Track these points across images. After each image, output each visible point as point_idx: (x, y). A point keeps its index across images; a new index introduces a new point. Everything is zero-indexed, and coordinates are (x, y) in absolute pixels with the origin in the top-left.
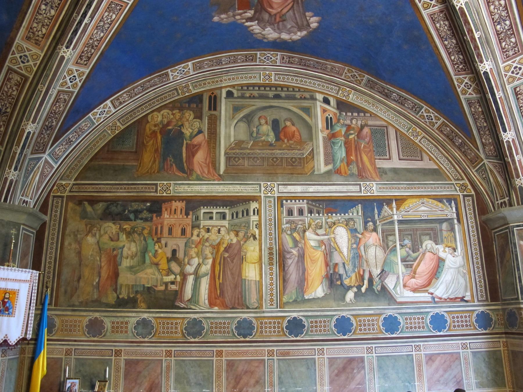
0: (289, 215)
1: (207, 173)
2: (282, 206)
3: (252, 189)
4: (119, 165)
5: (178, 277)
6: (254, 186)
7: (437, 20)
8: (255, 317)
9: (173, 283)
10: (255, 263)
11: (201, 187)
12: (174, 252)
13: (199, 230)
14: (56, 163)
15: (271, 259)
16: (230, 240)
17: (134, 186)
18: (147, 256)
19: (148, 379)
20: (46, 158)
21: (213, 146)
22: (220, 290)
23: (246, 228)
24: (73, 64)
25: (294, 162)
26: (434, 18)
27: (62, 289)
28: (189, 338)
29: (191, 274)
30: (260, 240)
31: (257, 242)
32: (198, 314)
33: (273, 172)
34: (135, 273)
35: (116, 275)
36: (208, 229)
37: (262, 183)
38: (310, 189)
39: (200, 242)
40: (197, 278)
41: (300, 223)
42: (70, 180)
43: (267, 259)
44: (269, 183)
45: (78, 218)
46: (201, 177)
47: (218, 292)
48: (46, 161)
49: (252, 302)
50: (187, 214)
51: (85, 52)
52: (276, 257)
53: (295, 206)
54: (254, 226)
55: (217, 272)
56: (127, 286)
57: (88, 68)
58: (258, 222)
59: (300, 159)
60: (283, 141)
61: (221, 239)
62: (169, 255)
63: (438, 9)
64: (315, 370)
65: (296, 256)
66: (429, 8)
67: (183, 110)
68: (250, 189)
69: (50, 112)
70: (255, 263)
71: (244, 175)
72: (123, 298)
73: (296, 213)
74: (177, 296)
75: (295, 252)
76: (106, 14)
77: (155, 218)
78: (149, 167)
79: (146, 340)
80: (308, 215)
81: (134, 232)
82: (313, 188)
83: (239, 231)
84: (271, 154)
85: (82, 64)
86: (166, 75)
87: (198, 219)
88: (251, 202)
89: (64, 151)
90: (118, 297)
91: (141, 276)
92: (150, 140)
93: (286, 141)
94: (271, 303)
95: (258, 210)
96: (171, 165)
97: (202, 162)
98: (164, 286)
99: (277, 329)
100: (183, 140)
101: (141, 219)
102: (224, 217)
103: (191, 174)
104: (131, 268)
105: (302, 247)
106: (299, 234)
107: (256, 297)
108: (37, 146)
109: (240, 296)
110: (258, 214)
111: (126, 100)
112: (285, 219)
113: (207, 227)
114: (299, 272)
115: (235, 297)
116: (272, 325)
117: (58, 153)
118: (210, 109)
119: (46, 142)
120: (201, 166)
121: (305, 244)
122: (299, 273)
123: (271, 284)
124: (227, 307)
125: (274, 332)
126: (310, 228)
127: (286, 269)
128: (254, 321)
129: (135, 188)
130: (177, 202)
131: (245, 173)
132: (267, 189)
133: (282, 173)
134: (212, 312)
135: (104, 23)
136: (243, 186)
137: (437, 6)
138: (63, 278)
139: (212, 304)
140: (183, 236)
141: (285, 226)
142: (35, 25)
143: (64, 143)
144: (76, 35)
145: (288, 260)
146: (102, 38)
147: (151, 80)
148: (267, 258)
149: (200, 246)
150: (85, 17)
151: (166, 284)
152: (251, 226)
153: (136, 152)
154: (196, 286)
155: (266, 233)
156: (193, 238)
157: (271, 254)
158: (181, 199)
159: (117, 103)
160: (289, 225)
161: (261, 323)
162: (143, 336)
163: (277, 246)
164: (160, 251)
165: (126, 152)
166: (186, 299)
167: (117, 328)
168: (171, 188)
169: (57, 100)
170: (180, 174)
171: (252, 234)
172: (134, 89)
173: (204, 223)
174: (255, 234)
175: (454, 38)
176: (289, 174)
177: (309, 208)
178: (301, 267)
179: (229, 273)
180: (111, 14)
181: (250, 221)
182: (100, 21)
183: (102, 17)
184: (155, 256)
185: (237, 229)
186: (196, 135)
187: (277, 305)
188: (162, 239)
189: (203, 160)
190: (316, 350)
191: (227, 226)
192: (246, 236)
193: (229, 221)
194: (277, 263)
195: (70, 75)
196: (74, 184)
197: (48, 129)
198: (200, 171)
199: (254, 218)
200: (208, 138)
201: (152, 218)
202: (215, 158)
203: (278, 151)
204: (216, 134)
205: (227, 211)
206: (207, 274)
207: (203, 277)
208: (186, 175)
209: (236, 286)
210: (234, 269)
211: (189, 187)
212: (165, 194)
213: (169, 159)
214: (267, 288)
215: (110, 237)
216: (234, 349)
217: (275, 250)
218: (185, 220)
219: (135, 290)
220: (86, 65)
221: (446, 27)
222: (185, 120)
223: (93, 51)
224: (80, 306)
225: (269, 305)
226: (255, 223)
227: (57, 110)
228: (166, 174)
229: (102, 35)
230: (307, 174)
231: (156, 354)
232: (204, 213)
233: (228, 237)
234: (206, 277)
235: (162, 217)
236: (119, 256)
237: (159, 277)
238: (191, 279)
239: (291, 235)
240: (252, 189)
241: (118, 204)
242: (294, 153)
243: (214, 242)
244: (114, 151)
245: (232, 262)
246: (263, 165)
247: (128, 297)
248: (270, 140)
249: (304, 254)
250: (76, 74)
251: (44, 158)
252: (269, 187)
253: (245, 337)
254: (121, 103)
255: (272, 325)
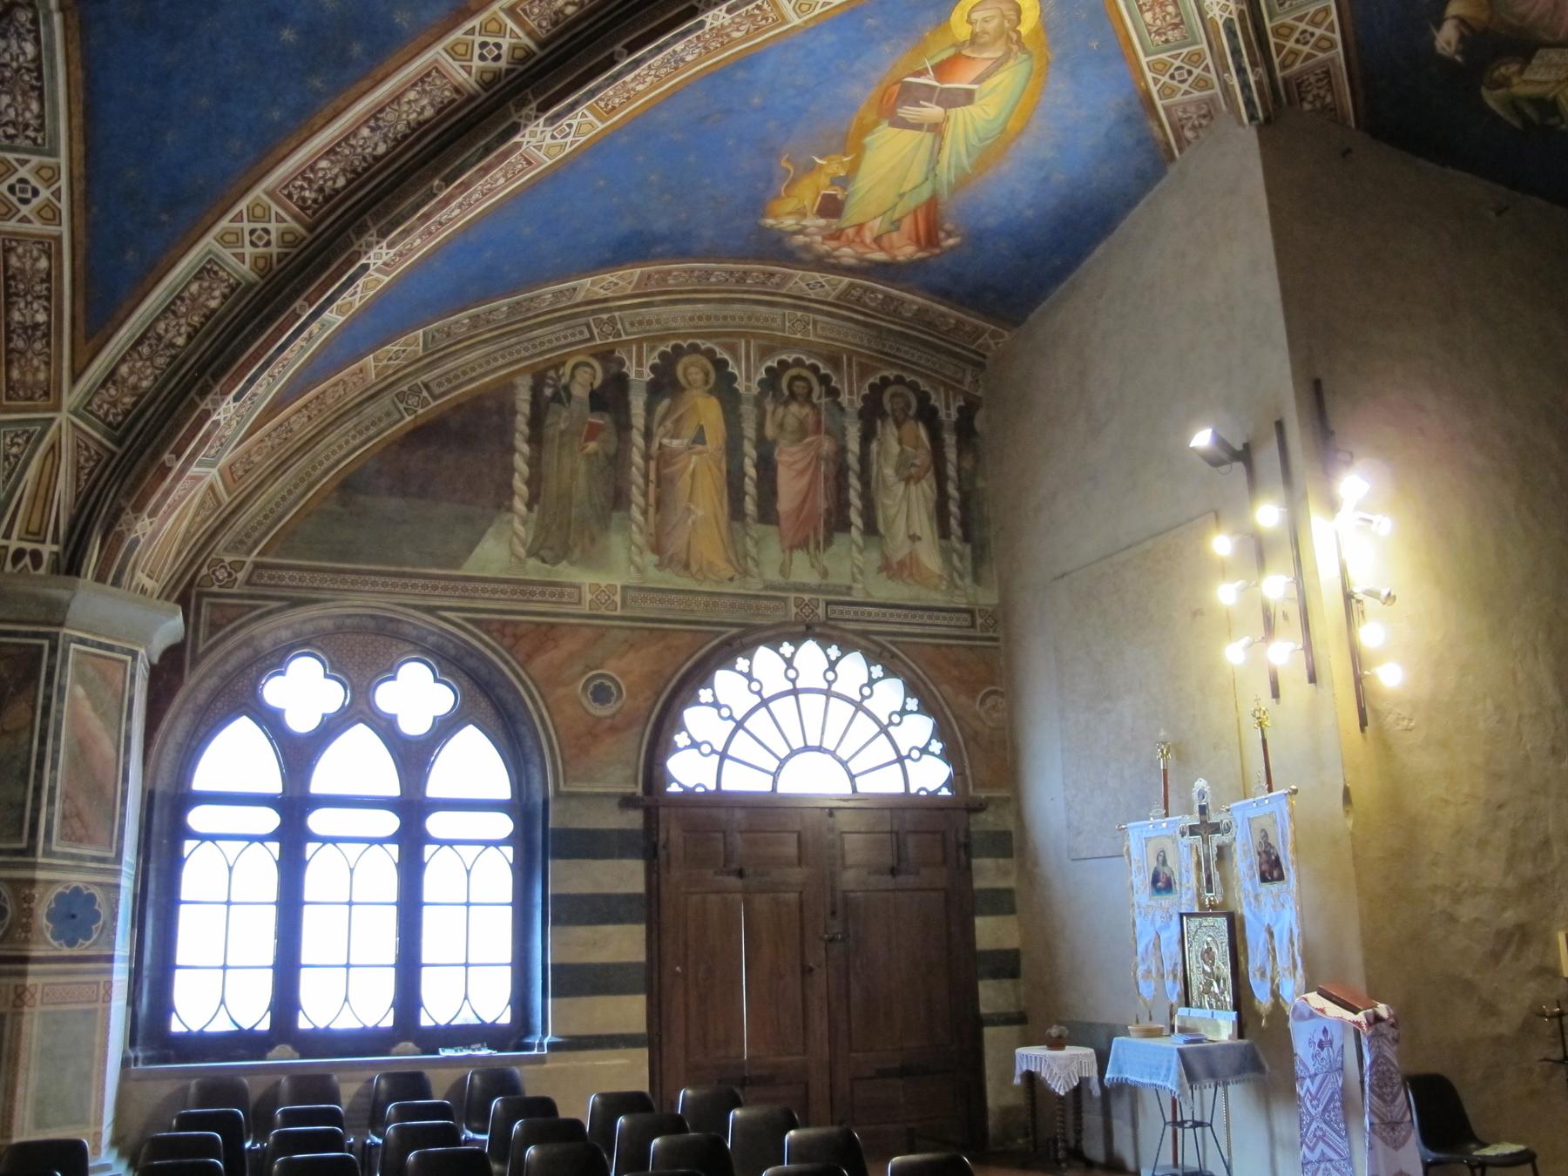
7: (428, 88)
26: (430, 80)
63: (460, 79)
66: (454, 59)
137: (470, 73)
175: (391, 144)
221: (414, 116)
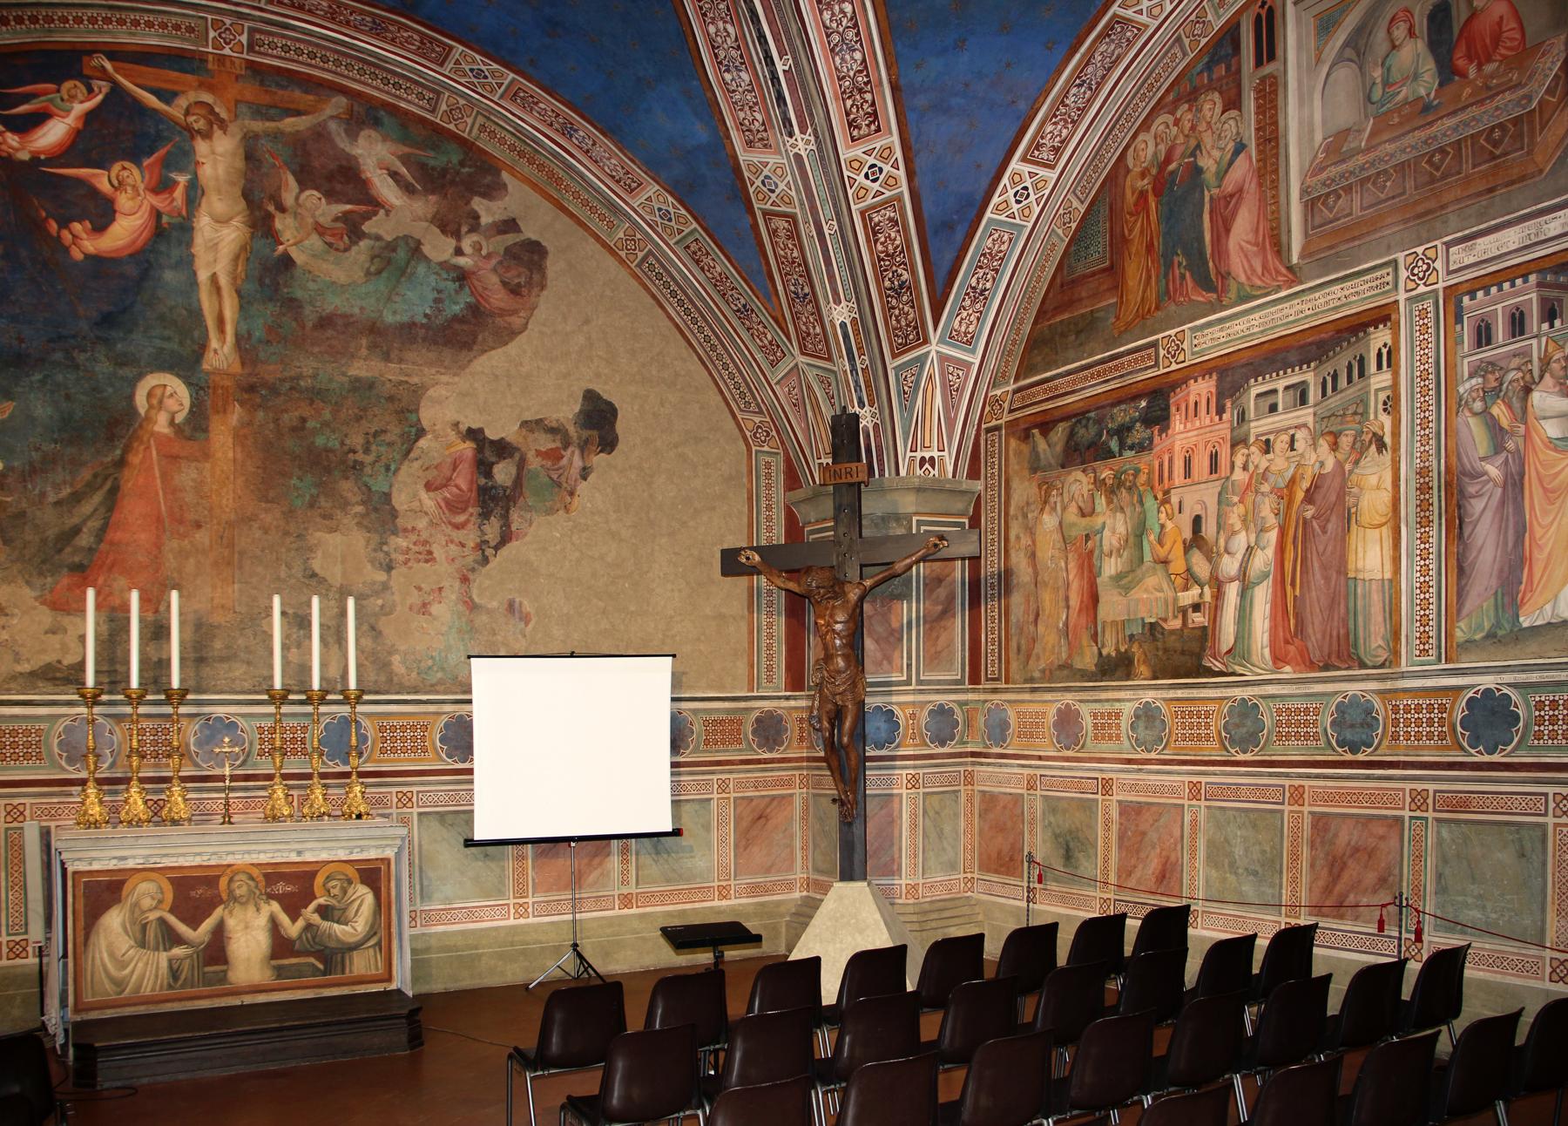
0: (1479, 345)
1: (1259, 270)
2: (1459, 319)
3: (1374, 284)
4: (1082, 315)
5: (1206, 589)
6: (1378, 274)
8: (1379, 692)
9: (1196, 607)
10: (1380, 526)
11: (1248, 321)
12: (1197, 521)
13: (1246, 451)
14: (973, 352)
15: (1424, 506)
16: (1318, 464)
17: (1115, 363)
18: (1145, 543)
19: (1158, 850)
20: (937, 352)
21: (1273, 181)
22: (1296, 615)
23: (1358, 418)
24: (848, 147)
25: (1496, 144)
27: (1013, 644)
28: (1233, 751)
29: (1232, 580)
30: (1396, 448)
31: (1387, 457)
32: (1249, 688)
33: (1432, 204)
34: (1127, 589)
35: (1094, 599)
36: (1268, 441)
37: (1400, 256)
38: (1552, 225)
39: (1249, 484)
40: (1245, 592)
41: (1516, 362)
42: (1007, 383)
43: (1412, 509)
44: (1420, 250)
45: (1026, 473)
46: (1248, 289)
47: (1292, 622)
48: (943, 358)
49: (1374, 645)
50: (1220, 411)
51: (854, 110)
52: (1439, 496)
53: (1499, 307)
54: (1380, 407)
55: (1288, 566)
56: (1114, 623)
57: (891, 133)
58: (1389, 392)
59: (1517, 121)
60: (1464, 75)
61: (1299, 465)
62: (1188, 534)
64: (1544, 864)
65: (1496, 485)
67: (1196, 99)
68: (1366, 286)
69: (877, 261)
70: (1380, 526)
71: (1352, 245)
72: (1109, 655)
73: (1500, 331)
74: (1206, 640)
75: (1493, 470)
76: (827, 16)
77: (1157, 439)
78: (1139, 299)
79: (1153, 755)
80: (1539, 328)
81: (1120, 484)
82: (1562, 221)
83: (1340, 433)
84: (1425, 142)
85: (869, 135)
86: (1118, 22)
87: (1243, 420)
88: (1372, 329)
89: (978, 319)
90: (1100, 654)
91: (1137, 596)
92: (1136, 221)
93: (1472, 71)
94: (1422, 647)
95: (1389, 353)
96: (1183, 277)
97: (1248, 242)
98: (1180, 616)
99: (1436, 729)
100: (1203, 192)
101: (1131, 448)
102: (1300, 395)
103: (1225, 290)
104: (1118, 578)
105: (1518, 451)
106: (1509, 407)
107: (1382, 629)
108: (897, 336)
109: (1342, 632)
110: (1389, 365)
111: (1064, 135)
112: (1466, 361)
113: (1264, 438)
114: (1505, 537)
115: (1331, 636)
116: (1424, 715)
117: (963, 329)
118: (1259, 63)
119: (915, 319)
120: (1246, 256)
121: (1527, 437)
122: (1505, 543)
123: (1424, 587)
124: (1312, 666)
125: (1430, 736)
126: (1547, 376)
127: (1466, 535)
128: (1377, 703)
129: (1116, 368)
130: (1200, 379)
131: (1354, 239)
132: (1416, 271)
133: (1458, 200)
134: (1279, 682)
135: (841, 35)
136: (1349, 284)
138: (1013, 619)
139: (1278, 659)
140: (1214, 476)
141: (1467, 385)
142: (742, 115)
143: (967, 303)
144: (785, 104)
145: (1472, 501)
146: (864, 60)
147: (1092, 56)
148: (1413, 503)
149: (1250, 497)
150: (773, 63)
151: (1183, 611)
152: (1372, 411)
153: (1111, 268)
154: (1245, 610)
155: (1413, 421)
156: (1234, 477)
157: (1424, 489)
158: (1204, 369)
159: (1045, 155)
160: (1480, 380)
161: (1396, 710)
162: (1149, 747)
163: (1443, 461)
164: (1169, 525)
165: (1093, 274)
166: (1224, 648)
167: (1106, 726)
168: (1185, 346)
169: (873, 231)
170: (1200, 297)
171: (1374, 434)
172: (1062, 102)
173: (1259, 426)
174: (1380, 433)
176: (1480, 194)
177: (1543, 301)
178: (1511, 518)
179: (1316, 565)
180: (837, 7)
181: (1368, 393)
182: (828, 36)
183: (825, 26)
184: (1160, 542)
185: (1333, 429)
186: (1231, 163)
187: (1440, 653)
188: (1173, 491)
189: (1251, 237)
190: (1551, 797)
191: (1311, 425)
192: (1358, 445)
193: (1315, 406)
194: (1440, 519)
195: (859, 170)
196: (1015, 392)
197: (899, 294)
198: (1245, 272)
199: (1379, 380)
200: (1258, 161)
201: (1151, 439)
202: (1278, 219)
203: (1450, 122)
204: (1277, 138)
205: (1309, 377)
206: (1266, 576)
207: (1258, 584)
208: (1215, 296)
209: (1333, 603)
210: (1330, 548)
211: (1221, 330)
212: (1174, 367)
213: (1176, 259)
214: (1412, 601)
215: (1080, 508)
216: (1321, 783)
217: (1435, 472)
218: (1217, 427)
219: (1128, 633)
220: (878, 130)
222: (1202, 127)
223: (868, 97)
224: (1042, 680)
225: (1418, 653)
226: (1382, 396)
227: (890, 247)
228: (1173, 307)
229: (858, 56)
230: (1541, 171)
231: (1173, 790)
232: (1258, 395)
233: (1314, 457)
234: (1265, 583)
235: (1170, 432)
236: (1097, 553)
237: (1170, 594)
238: (1232, 592)
239: (1485, 413)
240: (1374, 284)
241: (1089, 419)
242: (1497, 108)
243: (1280, 480)
244: (1073, 281)
245: (1324, 531)
246: (1403, 193)
247: (1117, 650)
248: (1423, 92)
249: (1522, 475)
250: (871, 161)
251: (933, 354)
252: (1420, 263)
253: (1354, 749)
254: (1057, 151)
255: (1424, 715)
